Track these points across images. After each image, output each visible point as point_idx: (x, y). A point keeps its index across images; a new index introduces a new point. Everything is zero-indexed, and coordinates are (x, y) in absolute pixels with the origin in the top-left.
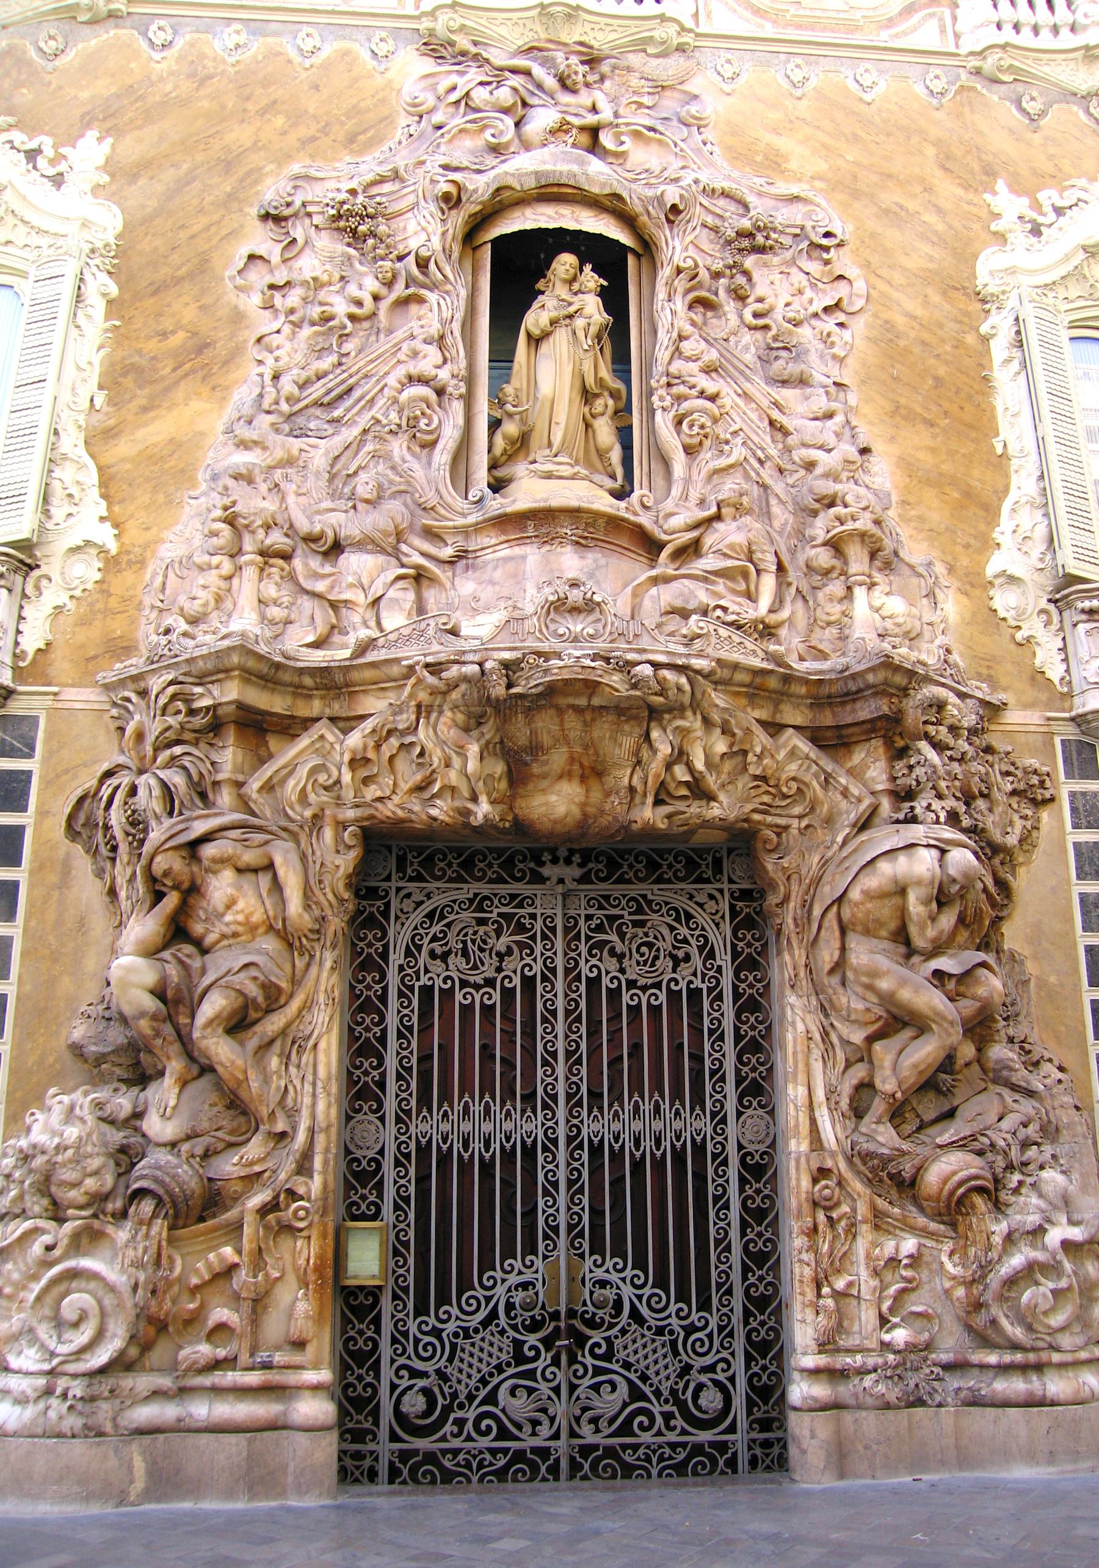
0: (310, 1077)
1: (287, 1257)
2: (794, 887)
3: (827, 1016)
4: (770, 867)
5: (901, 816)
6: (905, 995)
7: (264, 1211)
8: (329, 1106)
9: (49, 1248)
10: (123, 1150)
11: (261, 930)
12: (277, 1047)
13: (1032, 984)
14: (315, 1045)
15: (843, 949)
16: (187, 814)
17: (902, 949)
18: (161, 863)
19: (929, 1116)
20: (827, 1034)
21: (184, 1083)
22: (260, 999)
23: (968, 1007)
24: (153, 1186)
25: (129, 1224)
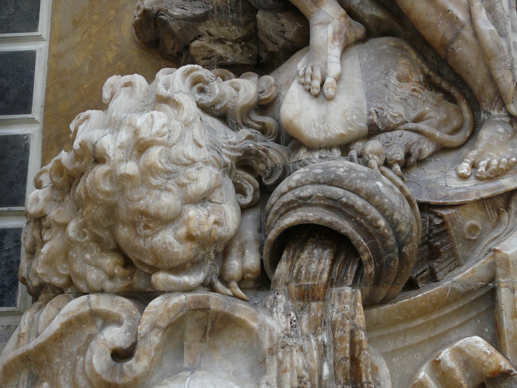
10: (246, 162)
24: (329, 217)
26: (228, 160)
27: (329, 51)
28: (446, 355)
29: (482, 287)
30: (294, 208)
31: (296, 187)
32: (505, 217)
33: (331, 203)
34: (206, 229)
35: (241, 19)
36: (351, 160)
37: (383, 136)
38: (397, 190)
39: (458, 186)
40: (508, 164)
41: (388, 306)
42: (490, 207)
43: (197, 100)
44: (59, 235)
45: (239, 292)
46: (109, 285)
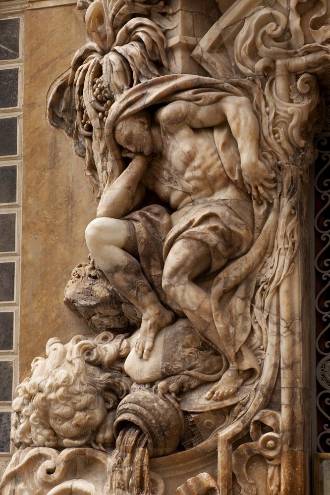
0: (274, 318)
1: (260, 482)
7: (235, 441)
8: (293, 344)
9: (50, 472)
11: (219, 183)
12: (241, 292)
14: (277, 289)
16: (143, 81)
18: (124, 129)
21: (158, 329)
22: (220, 247)
25: (116, 451)
26: (99, 389)
27: (147, 335)
28: (190, 480)
29: (212, 451)
30: (123, 413)
31: (125, 403)
32: (227, 419)
33: (135, 412)
34: (84, 421)
35: (115, 306)
36: (151, 391)
37: (169, 379)
38: (166, 406)
39: (202, 403)
40: (228, 393)
41: (165, 457)
42: (219, 413)
43: (86, 359)
44: (26, 421)
45: (102, 448)
46: (47, 443)
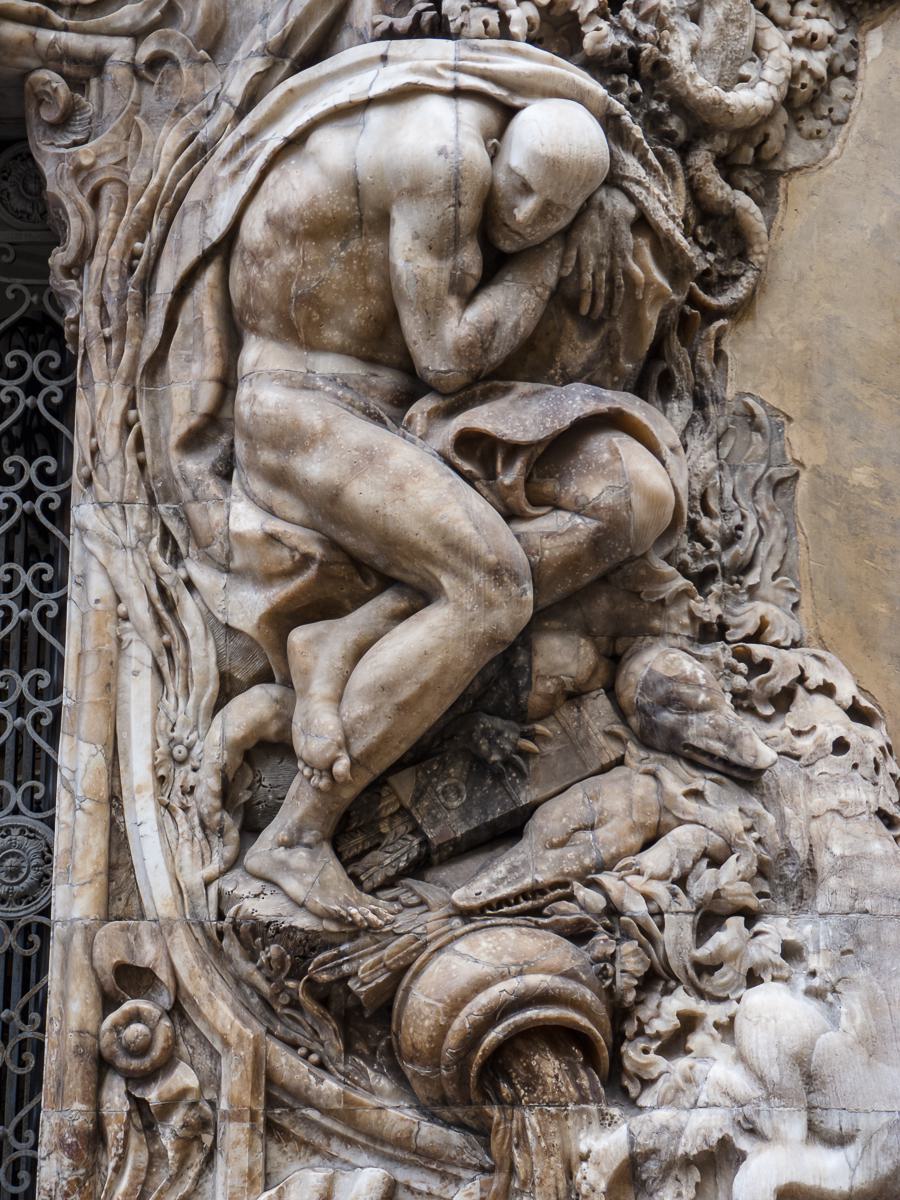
2: (107, 219)
3: (177, 559)
4: (49, 169)
5: (403, 22)
6: (364, 494)
13: (802, 486)
15: (228, 383)
17: (386, 379)
19: (452, 823)
20: (172, 607)
23: (557, 531)
